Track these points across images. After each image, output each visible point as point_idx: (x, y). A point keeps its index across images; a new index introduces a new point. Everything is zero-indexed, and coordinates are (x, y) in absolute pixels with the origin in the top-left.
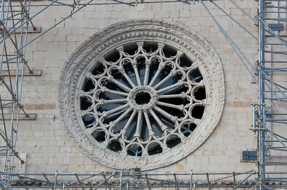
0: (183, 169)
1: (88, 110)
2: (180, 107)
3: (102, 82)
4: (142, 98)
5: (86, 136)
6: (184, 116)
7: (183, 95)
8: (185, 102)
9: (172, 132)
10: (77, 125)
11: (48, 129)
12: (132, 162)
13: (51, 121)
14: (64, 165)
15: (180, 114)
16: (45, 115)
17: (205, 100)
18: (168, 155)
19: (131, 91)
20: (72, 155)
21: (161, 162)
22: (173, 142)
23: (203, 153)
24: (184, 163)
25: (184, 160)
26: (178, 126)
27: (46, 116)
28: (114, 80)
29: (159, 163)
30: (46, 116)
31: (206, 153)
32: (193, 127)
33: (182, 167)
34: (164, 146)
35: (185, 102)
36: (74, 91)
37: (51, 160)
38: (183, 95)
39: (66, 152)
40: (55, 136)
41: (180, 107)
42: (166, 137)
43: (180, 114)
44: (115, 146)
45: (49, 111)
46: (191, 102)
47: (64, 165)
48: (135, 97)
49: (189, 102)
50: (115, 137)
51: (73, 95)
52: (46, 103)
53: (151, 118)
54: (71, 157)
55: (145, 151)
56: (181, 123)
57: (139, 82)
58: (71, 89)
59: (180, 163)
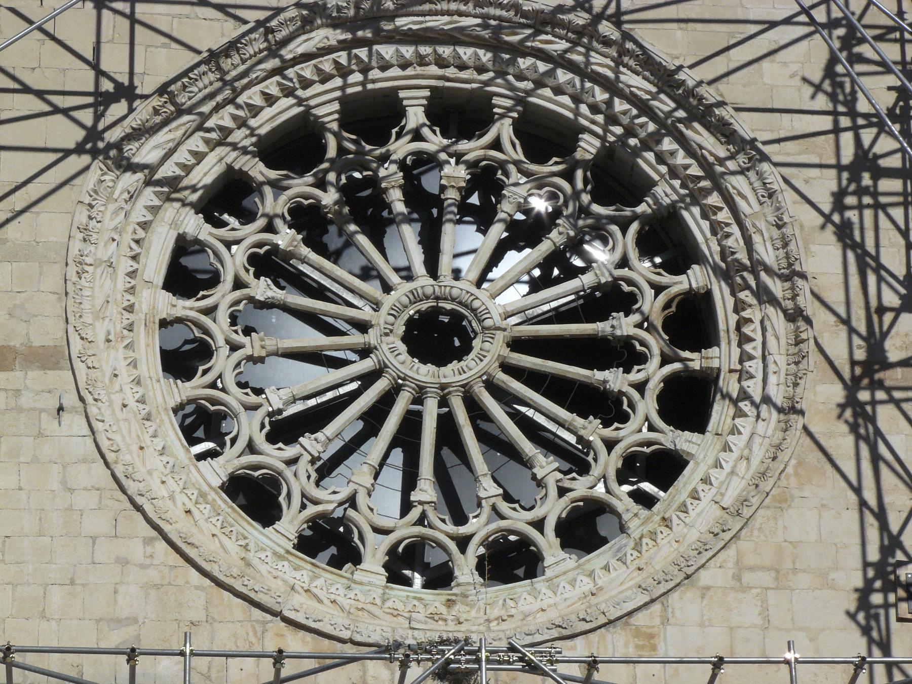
0: (654, 648)
1: (197, 380)
2: (614, 379)
3: (253, 260)
4: (438, 334)
5: (202, 495)
6: (624, 418)
7: (624, 325)
8: (626, 354)
9: (581, 486)
10: (159, 443)
11: (35, 460)
12: (414, 613)
13: (49, 423)
14: (119, 622)
15: (610, 408)
16: (17, 392)
17: (714, 351)
18: (566, 585)
19: (388, 301)
20: (153, 575)
21: (553, 615)
22: (584, 529)
23: (738, 578)
24: (657, 621)
25: (656, 607)
26: (608, 463)
27: (26, 400)
28: (305, 251)
29: (542, 618)
30: (26, 400)
31: (747, 578)
32: (664, 467)
33: (651, 636)
34: (548, 544)
35: (626, 354)
36: (131, 290)
37: (56, 596)
38: (624, 325)
39: (123, 562)
40: (71, 490)
41: (614, 379)
42: (554, 509)
43: (610, 408)
44: (329, 540)
45: (35, 377)
46: (656, 361)
47: (119, 622)
48: (401, 329)
49: (642, 359)
50: (329, 497)
51: (130, 309)
52: (16, 343)
53: (447, 430)
54: (149, 587)
55: (465, 568)
56: (619, 449)
57: (419, 268)
58: (122, 282)
59: (640, 619)
